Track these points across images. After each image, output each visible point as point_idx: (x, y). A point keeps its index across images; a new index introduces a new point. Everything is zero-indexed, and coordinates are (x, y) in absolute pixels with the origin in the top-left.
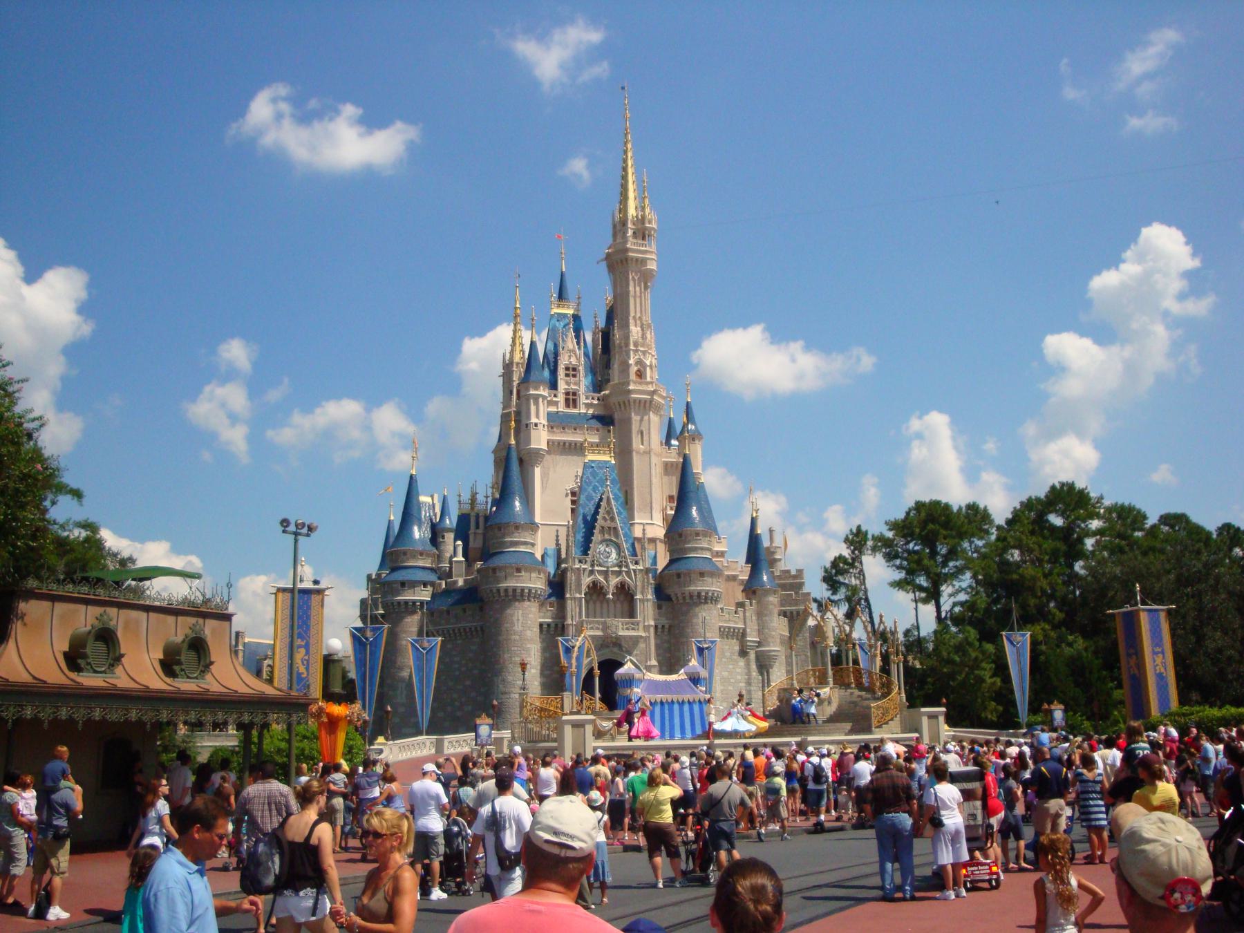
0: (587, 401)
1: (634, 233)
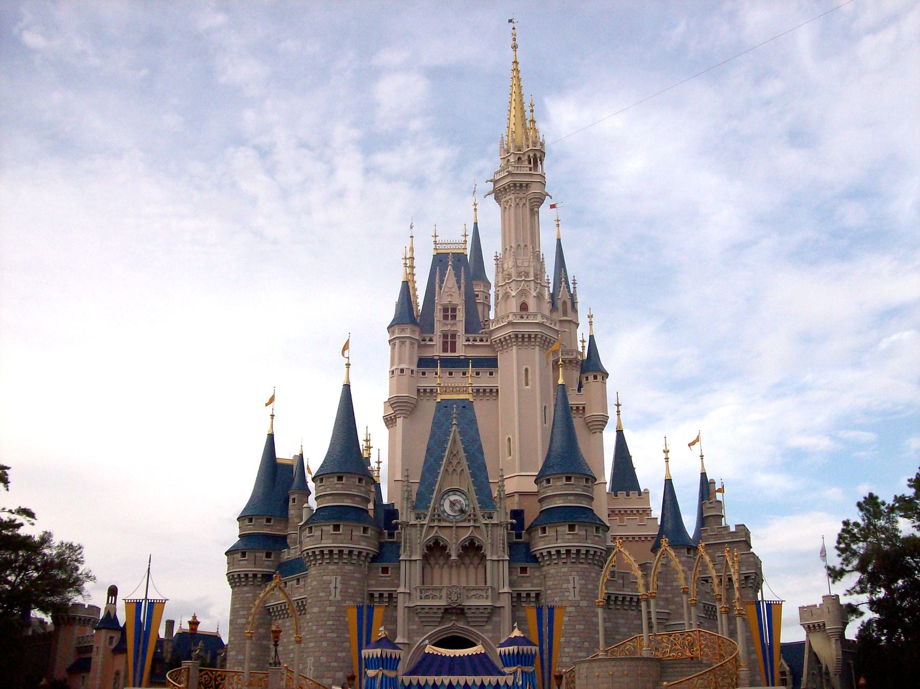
0: (467, 343)
1: (519, 159)
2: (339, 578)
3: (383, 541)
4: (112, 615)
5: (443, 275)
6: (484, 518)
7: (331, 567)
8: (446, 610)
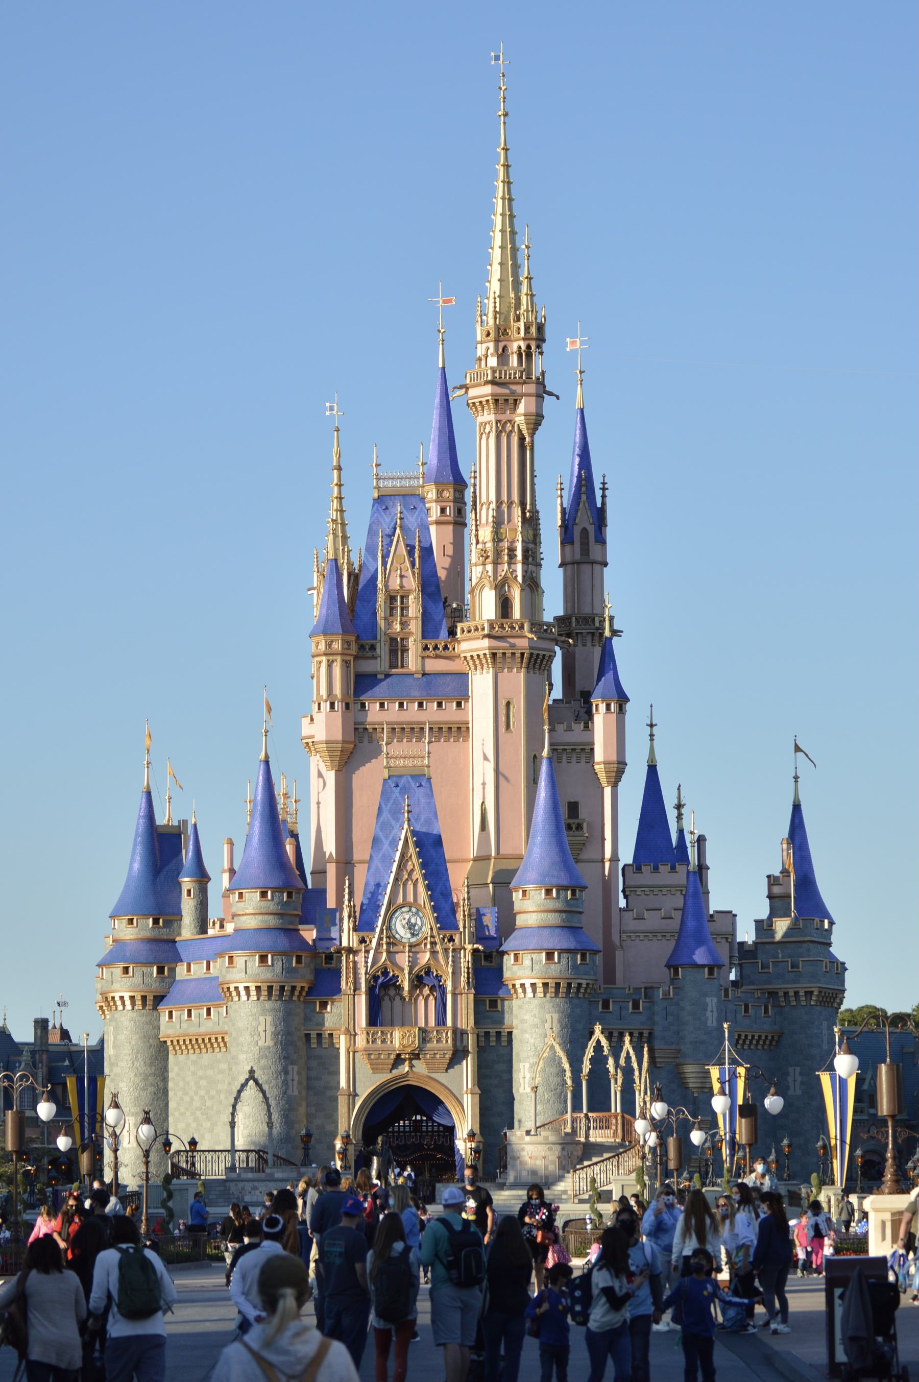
2: (269, 1019)
8: (398, 1055)
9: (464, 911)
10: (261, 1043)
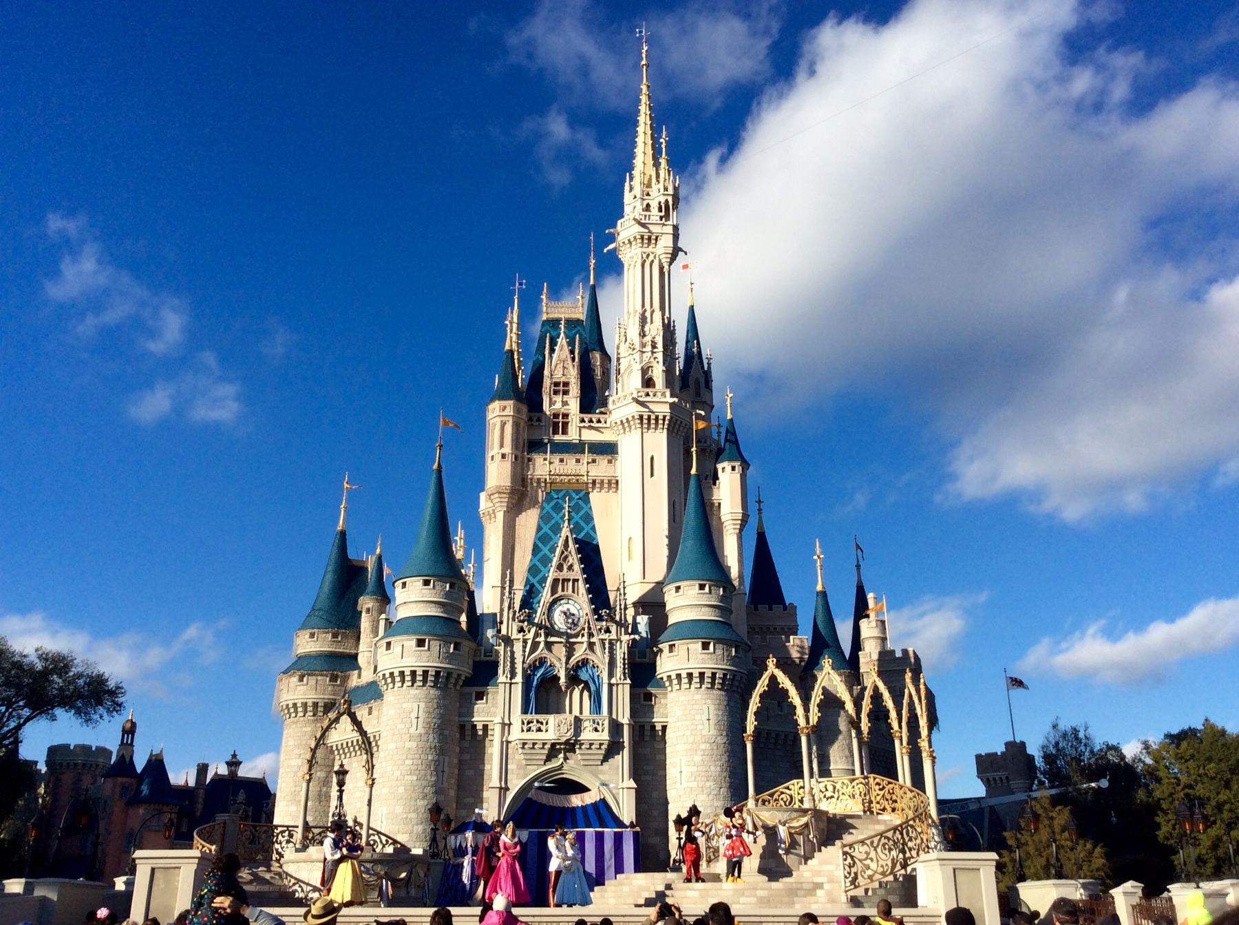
1: (648, 205)
2: (422, 705)
3: (477, 659)
4: (128, 759)
5: (553, 343)
6: (601, 632)
7: (413, 691)
8: (553, 745)
9: (620, 605)
10: (412, 730)
